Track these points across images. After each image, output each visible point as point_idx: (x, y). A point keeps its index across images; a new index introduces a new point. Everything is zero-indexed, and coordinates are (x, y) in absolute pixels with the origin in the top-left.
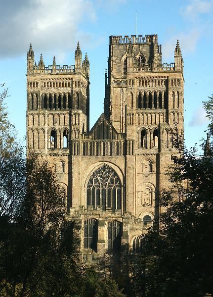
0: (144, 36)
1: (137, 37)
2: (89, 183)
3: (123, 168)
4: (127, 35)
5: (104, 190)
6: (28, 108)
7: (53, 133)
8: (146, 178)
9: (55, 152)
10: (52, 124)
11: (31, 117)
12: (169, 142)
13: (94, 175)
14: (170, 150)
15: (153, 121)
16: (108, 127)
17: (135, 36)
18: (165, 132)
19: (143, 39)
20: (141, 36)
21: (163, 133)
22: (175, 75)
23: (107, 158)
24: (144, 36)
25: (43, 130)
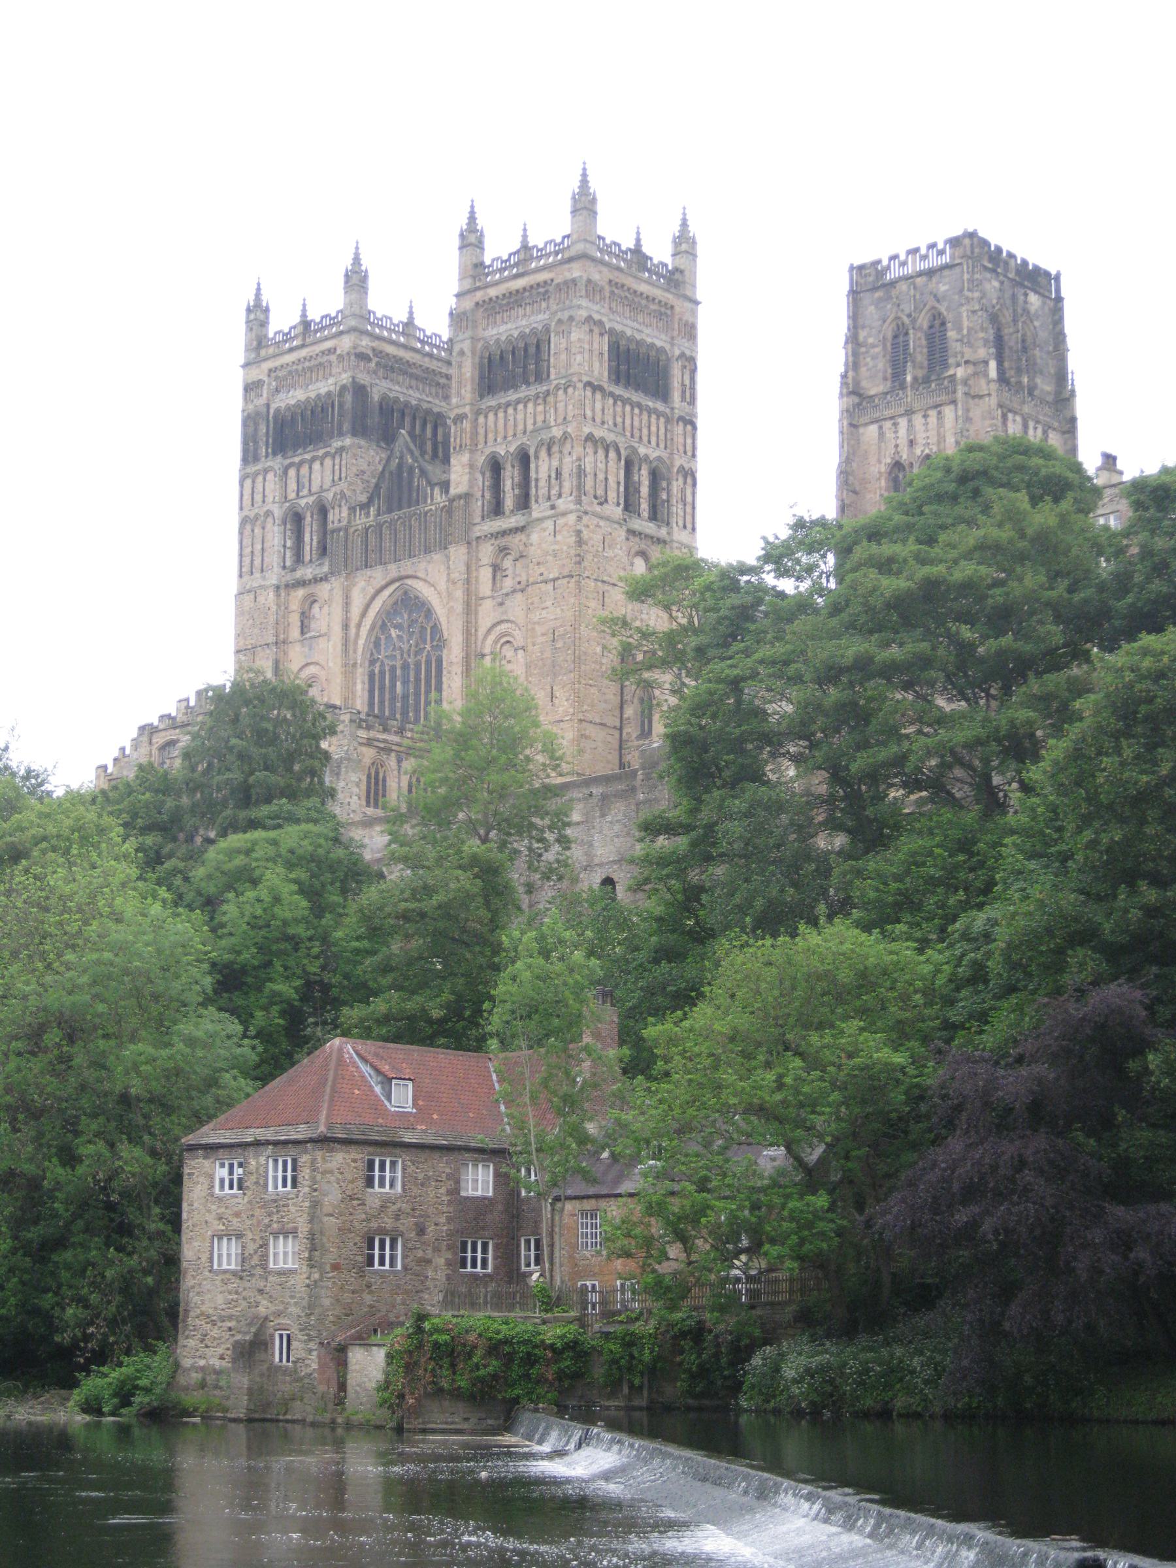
0: (940, 246)
1: (923, 251)
2: (372, 654)
3: (442, 585)
4: (892, 253)
5: (405, 667)
6: (245, 460)
7: (296, 519)
8: (501, 609)
9: (298, 574)
10: (292, 495)
11: (248, 482)
12: (553, 481)
13: (384, 626)
14: (553, 507)
15: (521, 427)
16: (411, 470)
17: (917, 250)
18: (543, 454)
19: (941, 253)
20: (932, 246)
21: (537, 457)
22: (569, 270)
23: (407, 567)
24: (940, 246)
25: (268, 513)
